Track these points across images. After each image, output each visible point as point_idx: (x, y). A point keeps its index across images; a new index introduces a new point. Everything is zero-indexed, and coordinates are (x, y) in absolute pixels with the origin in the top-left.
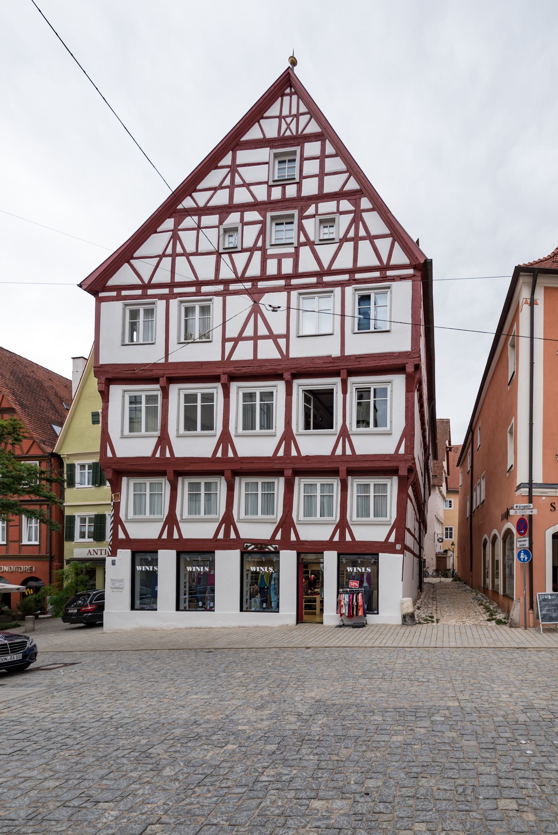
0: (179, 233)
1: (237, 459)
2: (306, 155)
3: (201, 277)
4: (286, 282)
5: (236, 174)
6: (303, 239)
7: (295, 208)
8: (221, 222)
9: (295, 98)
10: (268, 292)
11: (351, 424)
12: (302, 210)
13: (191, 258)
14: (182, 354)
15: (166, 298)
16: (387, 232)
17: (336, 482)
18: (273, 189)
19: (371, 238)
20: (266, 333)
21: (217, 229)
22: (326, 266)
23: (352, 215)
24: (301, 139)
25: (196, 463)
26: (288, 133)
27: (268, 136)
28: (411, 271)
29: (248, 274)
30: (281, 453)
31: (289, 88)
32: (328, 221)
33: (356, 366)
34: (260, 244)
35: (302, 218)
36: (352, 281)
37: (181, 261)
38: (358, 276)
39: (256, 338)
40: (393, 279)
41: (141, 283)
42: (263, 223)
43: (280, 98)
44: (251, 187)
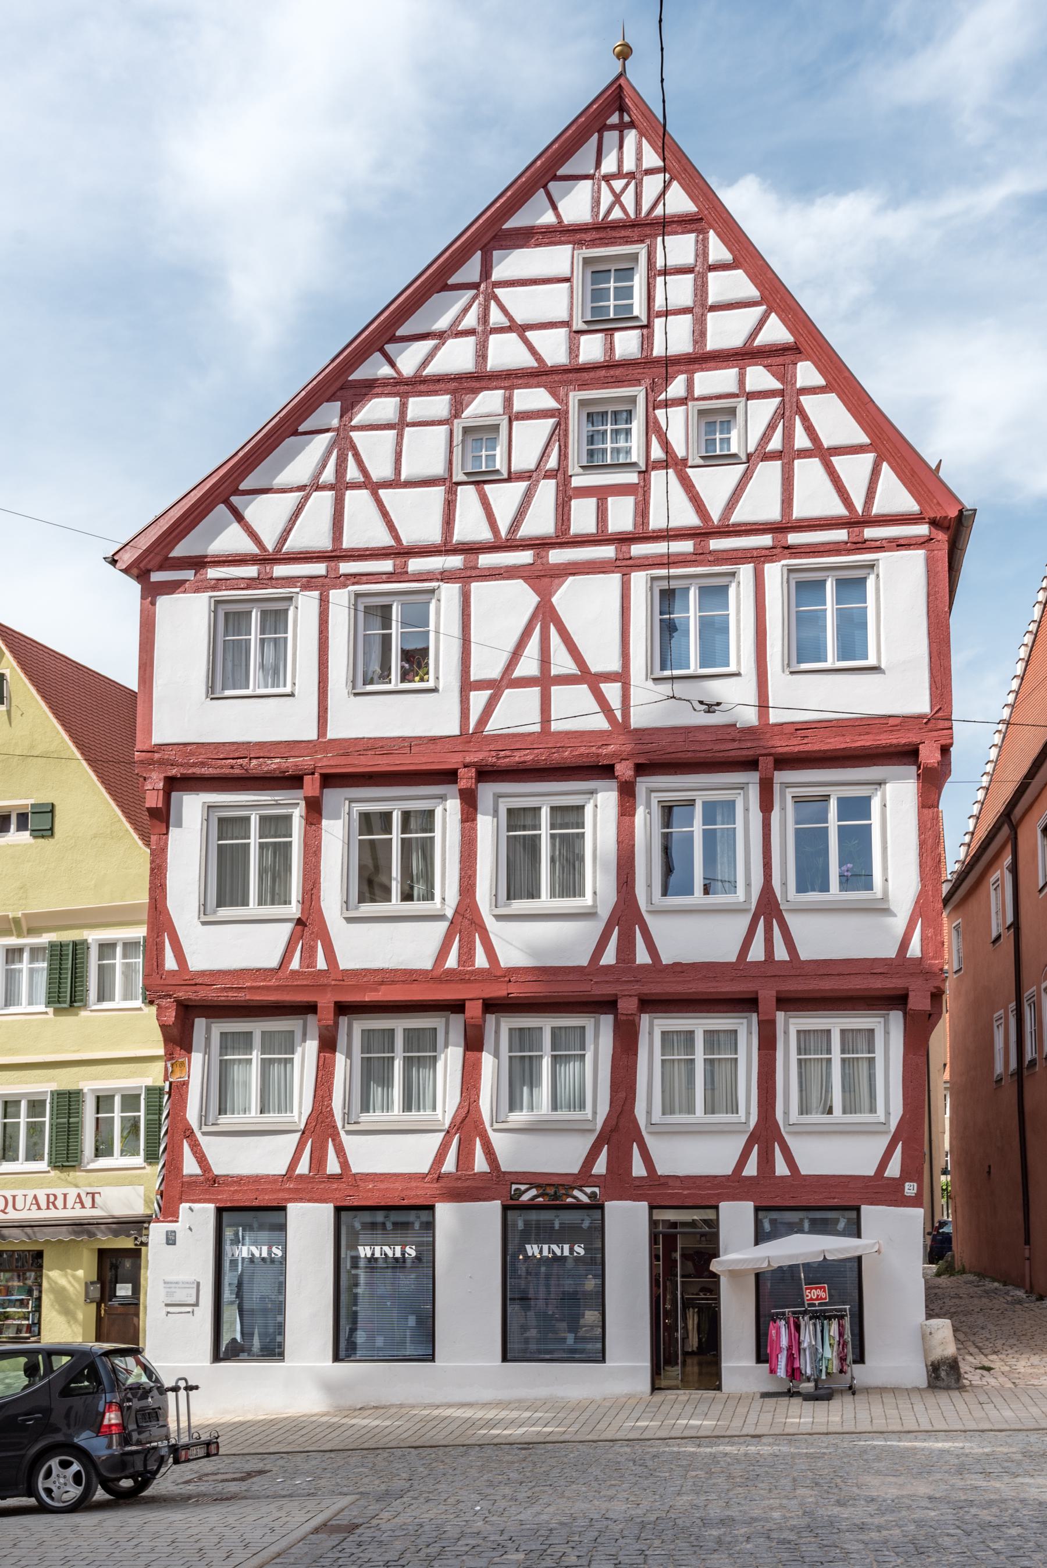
3: (408, 538)
5: (493, 303)
6: (657, 452)
7: (637, 382)
8: (457, 410)
10: (574, 574)
11: (784, 884)
13: (382, 492)
16: (863, 439)
17: (744, 1029)
18: (584, 339)
19: (824, 454)
22: (715, 515)
25: (393, 983)
26: (617, 214)
27: (567, 219)
28: (922, 530)
30: (609, 958)
31: (617, 113)
32: (716, 417)
33: (796, 749)
34: (552, 463)
35: (653, 405)
37: (357, 501)
38: (794, 538)
39: (545, 681)
40: (880, 546)
42: (560, 416)
43: (596, 135)
44: (529, 334)
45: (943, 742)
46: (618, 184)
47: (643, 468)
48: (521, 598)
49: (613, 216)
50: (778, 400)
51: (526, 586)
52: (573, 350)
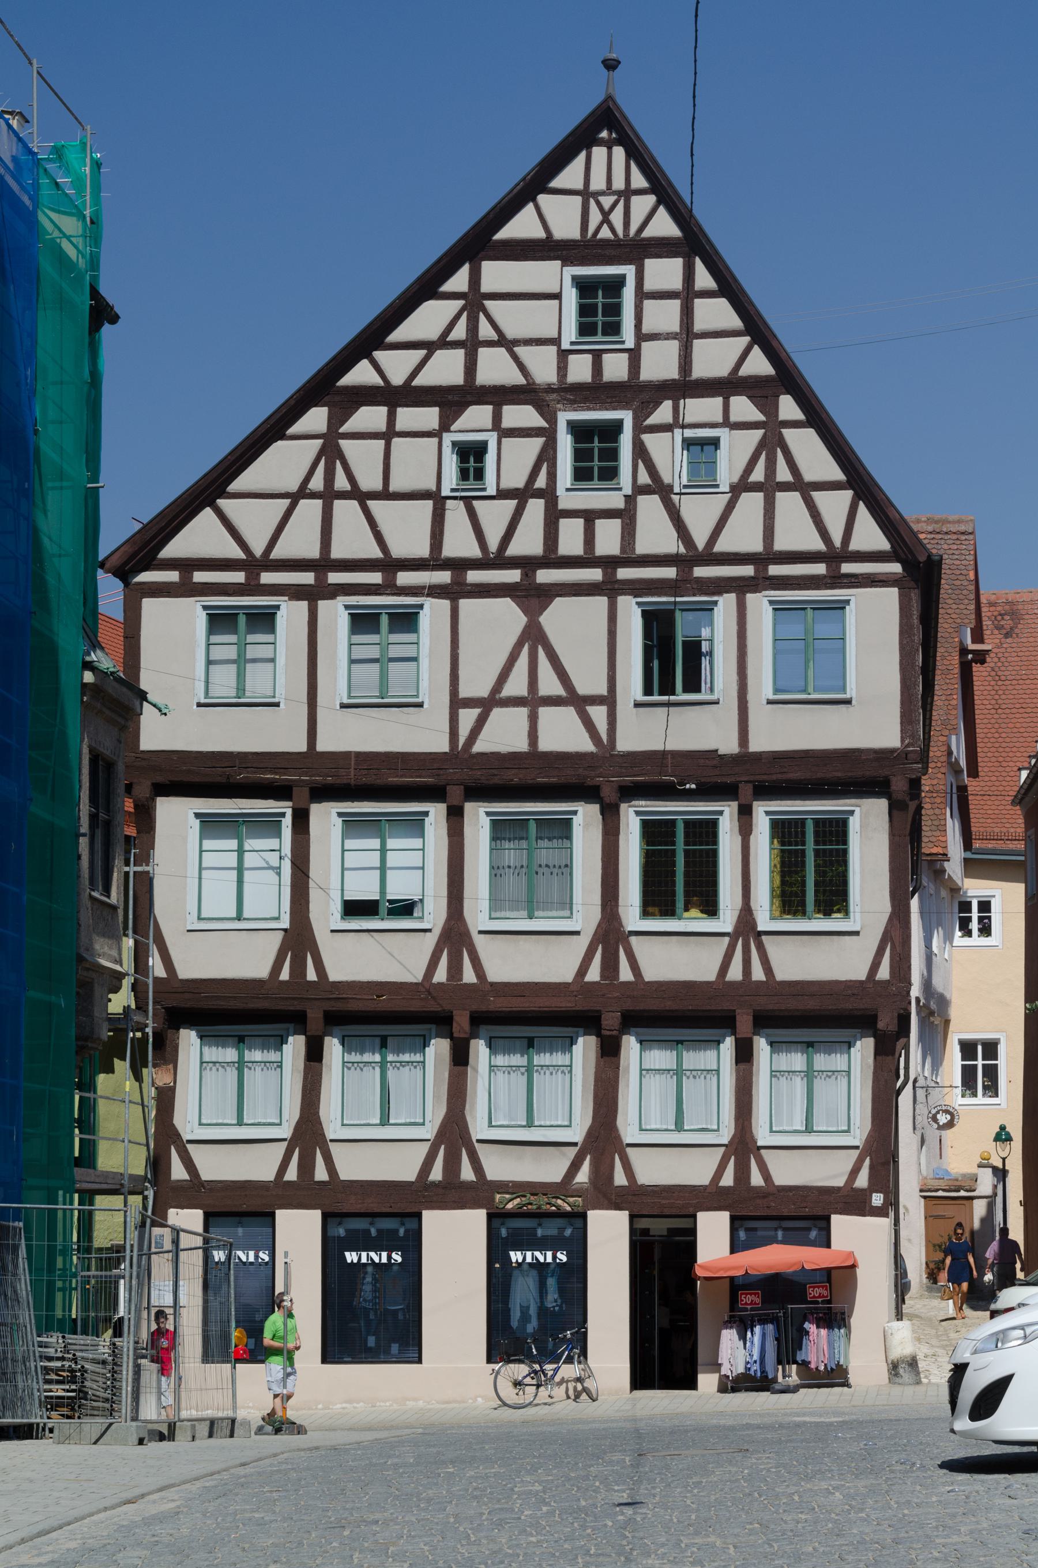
0: (344, 443)
1: (485, 987)
2: (649, 286)
4: (605, 575)
5: (482, 316)
6: (644, 478)
9: (619, 152)
10: (561, 596)
15: (311, 595)
18: (572, 358)
20: (559, 690)
22: (700, 543)
23: (759, 433)
24: (638, 249)
26: (605, 233)
29: (514, 549)
34: (541, 482)
35: (640, 429)
36: (760, 582)
37: (346, 511)
38: (774, 570)
41: (243, 556)
42: (549, 435)
46: (607, 201)
47: (630, 493)
49: (600, 236)
50: (761, 432)
52: (562, 368)
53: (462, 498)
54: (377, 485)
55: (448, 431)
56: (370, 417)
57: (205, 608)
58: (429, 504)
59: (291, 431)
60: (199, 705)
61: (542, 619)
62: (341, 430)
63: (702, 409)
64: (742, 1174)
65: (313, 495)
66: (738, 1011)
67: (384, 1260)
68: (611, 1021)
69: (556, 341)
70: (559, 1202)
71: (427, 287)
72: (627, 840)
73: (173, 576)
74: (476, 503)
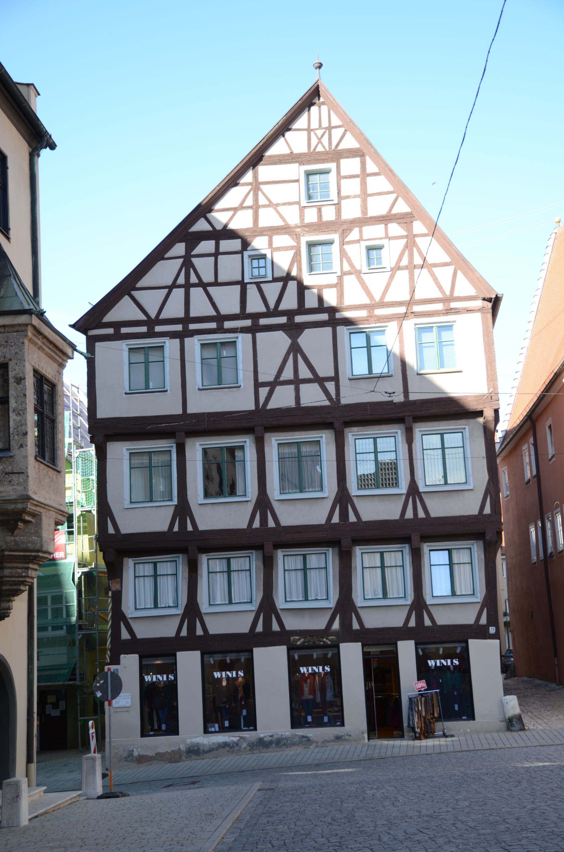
0: (193, 260)
1: (280, 529)
3: (224, 311)
4: (329, 316)
5: (260, 192)
6: (346, 268)
7: (335, 231)
10: (308, 328)
12: (344, 234)
14: (202, 403)
15: (181, 336)
20: (310, 375)
21: (240, 255)
23: (405, 240)
24: (336, 155)
26: (320, 149)
27: (296, 151)
29: (282, 307)
35: (342, 243)
37: (197, 293)
38: (416, 308)
45: (496, 408)
48: (281, 340)
49: (317, 150)
50: (405, 240)
51: (284, 334)
52: (302, 216)
53: (255, 283)
54: (211, 279)
55: (246, 250)
56: (207, 246)
57: (127, 345)
58: (238, 287)
59: (166, 256)
60: (126, 394)
61: (299, 340)
62: (192, 253)
63: (373, 232)
64: (420, 619)
65: (180, 286)
66: (412, 534)
67: (234, 675)
68: (345, 542)
69: (298, 203)
70: (325, 639)
71: (233, 181)
72: (349, 450)
73: (111, 331)
74: (262, 285)
